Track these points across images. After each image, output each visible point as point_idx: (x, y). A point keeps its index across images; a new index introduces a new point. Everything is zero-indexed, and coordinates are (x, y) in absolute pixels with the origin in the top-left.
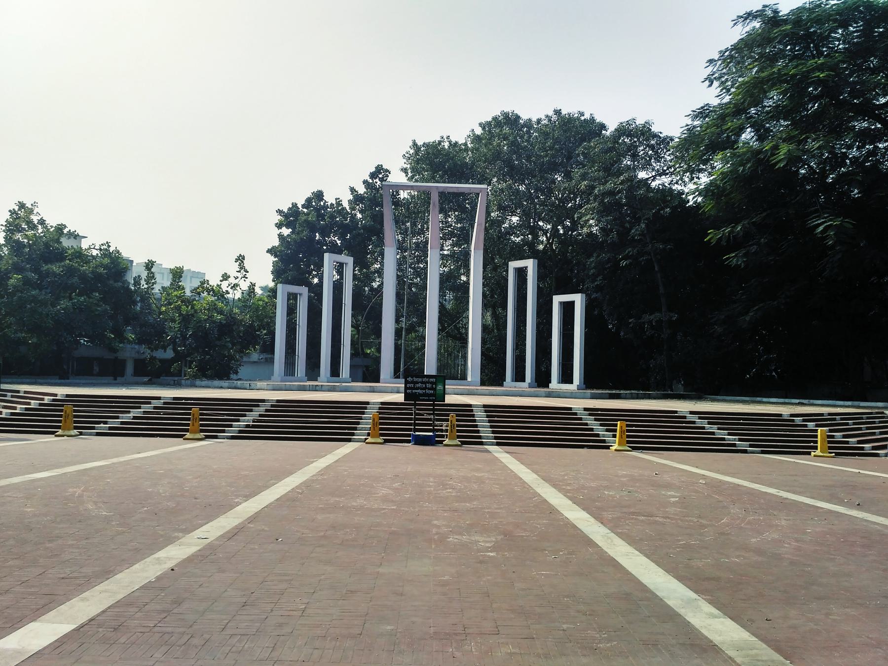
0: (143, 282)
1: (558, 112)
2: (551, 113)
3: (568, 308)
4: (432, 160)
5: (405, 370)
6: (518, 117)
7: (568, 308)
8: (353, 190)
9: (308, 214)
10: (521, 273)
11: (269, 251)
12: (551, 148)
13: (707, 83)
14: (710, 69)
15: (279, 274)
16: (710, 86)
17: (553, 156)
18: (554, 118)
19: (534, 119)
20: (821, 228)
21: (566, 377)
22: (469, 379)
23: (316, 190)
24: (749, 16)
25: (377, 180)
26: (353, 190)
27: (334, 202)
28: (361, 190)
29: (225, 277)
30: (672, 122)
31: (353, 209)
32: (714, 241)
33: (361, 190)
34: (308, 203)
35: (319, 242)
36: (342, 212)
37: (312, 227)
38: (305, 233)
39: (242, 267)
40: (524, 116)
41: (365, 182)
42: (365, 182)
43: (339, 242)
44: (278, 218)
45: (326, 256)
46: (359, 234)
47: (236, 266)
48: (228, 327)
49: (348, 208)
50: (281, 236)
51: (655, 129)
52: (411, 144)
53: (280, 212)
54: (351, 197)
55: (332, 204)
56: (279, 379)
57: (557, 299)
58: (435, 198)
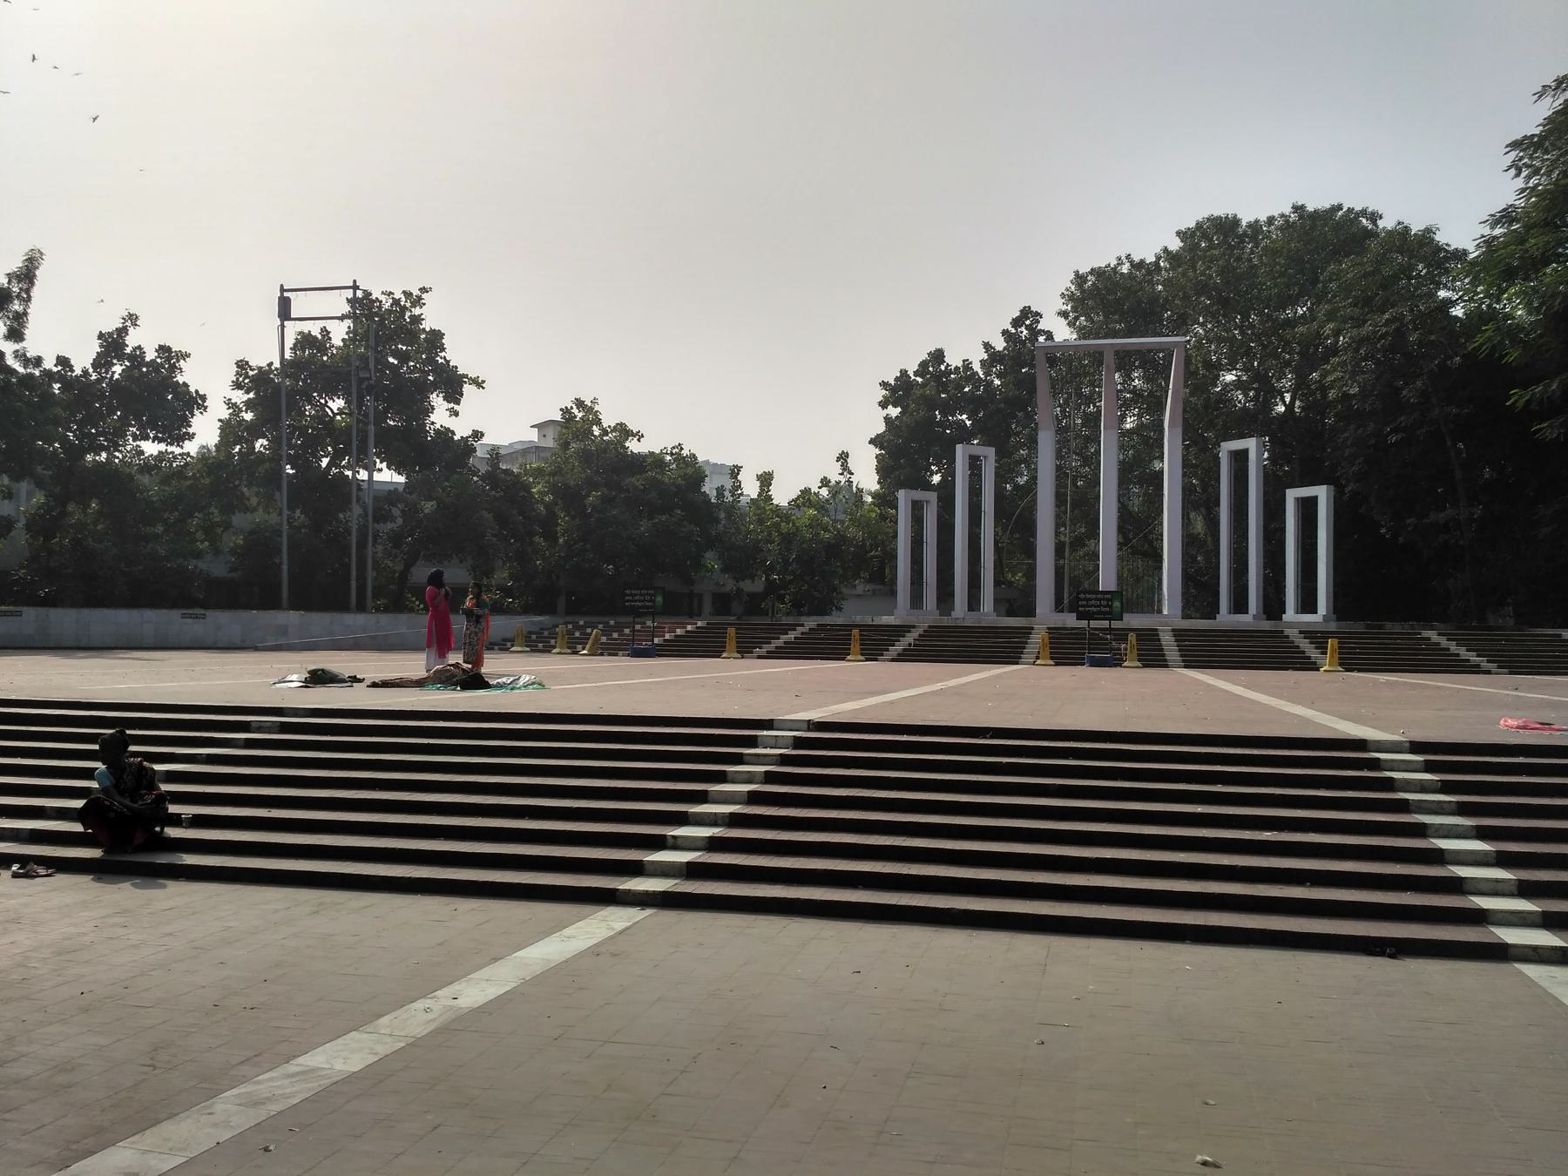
0: (727, 493)
1: (1298, 209)
2: (1287, 210)
3: (1308, 508)
4: (1108, 297)
6: (1235, 222)
8: (987, 346)
9: (923, 385)
10: (1240, 457)
11: (871, 442)
12: (1282, 275)
13: (1513, 172)
14: (1513, 155)
15: (884, 470)
16: (1518, 175)
17: (1288, 286)
18: (1293, 217)
19: (1263, 218)
22: (1165, 612)
26: (987, 346)
27: (960, 364)
28: (1000, 344)
29: (825, 482)
30: (1463, 231)
31: (987, 374)
33: (1000, 344)
34: (923, 369)
35: (940, 424)
37: (931, 403)
39: (845, 468)
40: (1246, 218)
41: (1005, 332)
42: (1005, 332)
43: (968, 423)
45: (959, 447)
47: (838, 467)
48: (835, 548)
50: (887, 419)
51: (1441, 238)
52: (1072, 276)
53: (884, 385)
55: (957, 368)
57: (1292, 495)
58: (1109, 359)
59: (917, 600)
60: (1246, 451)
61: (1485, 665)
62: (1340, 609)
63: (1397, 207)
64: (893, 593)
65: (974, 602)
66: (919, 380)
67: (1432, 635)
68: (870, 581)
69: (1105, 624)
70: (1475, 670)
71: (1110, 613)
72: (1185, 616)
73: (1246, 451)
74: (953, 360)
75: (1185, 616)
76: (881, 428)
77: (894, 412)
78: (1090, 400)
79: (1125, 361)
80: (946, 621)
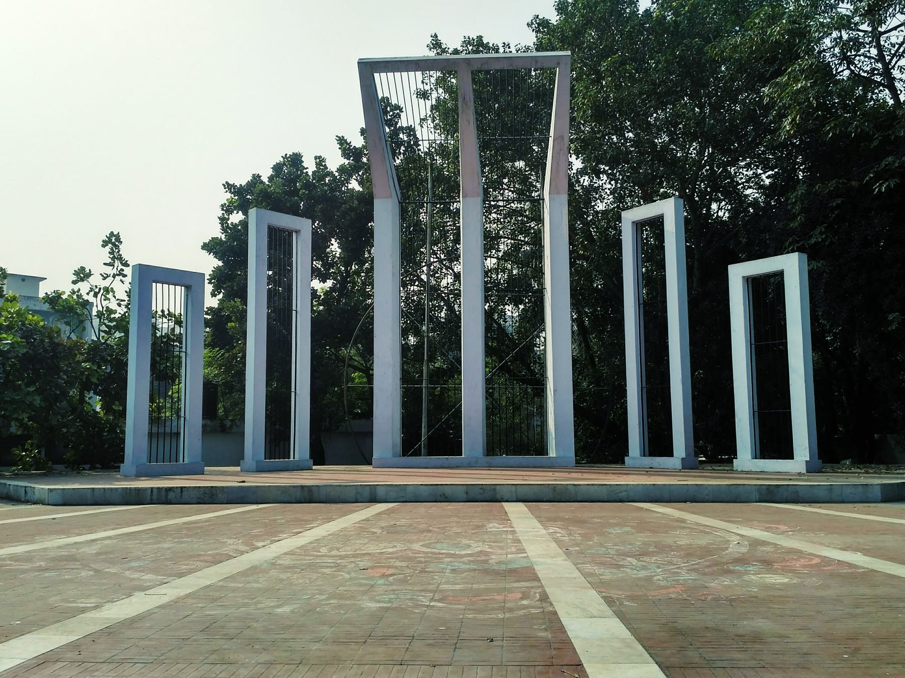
5: (429, 438)
8: (342, 141)
11: (205, 247)
21: (774, 440)
22: (552, 453)
23: (290, 153)
26: (342, 141)
29: (82, 275)
39: (116, 257)
44: (226, 197)
46: (352, 209)
47: (105, 254)
49: (337, 174)
53: (229, 187)
56: (133, 471)
74: (310, 166)
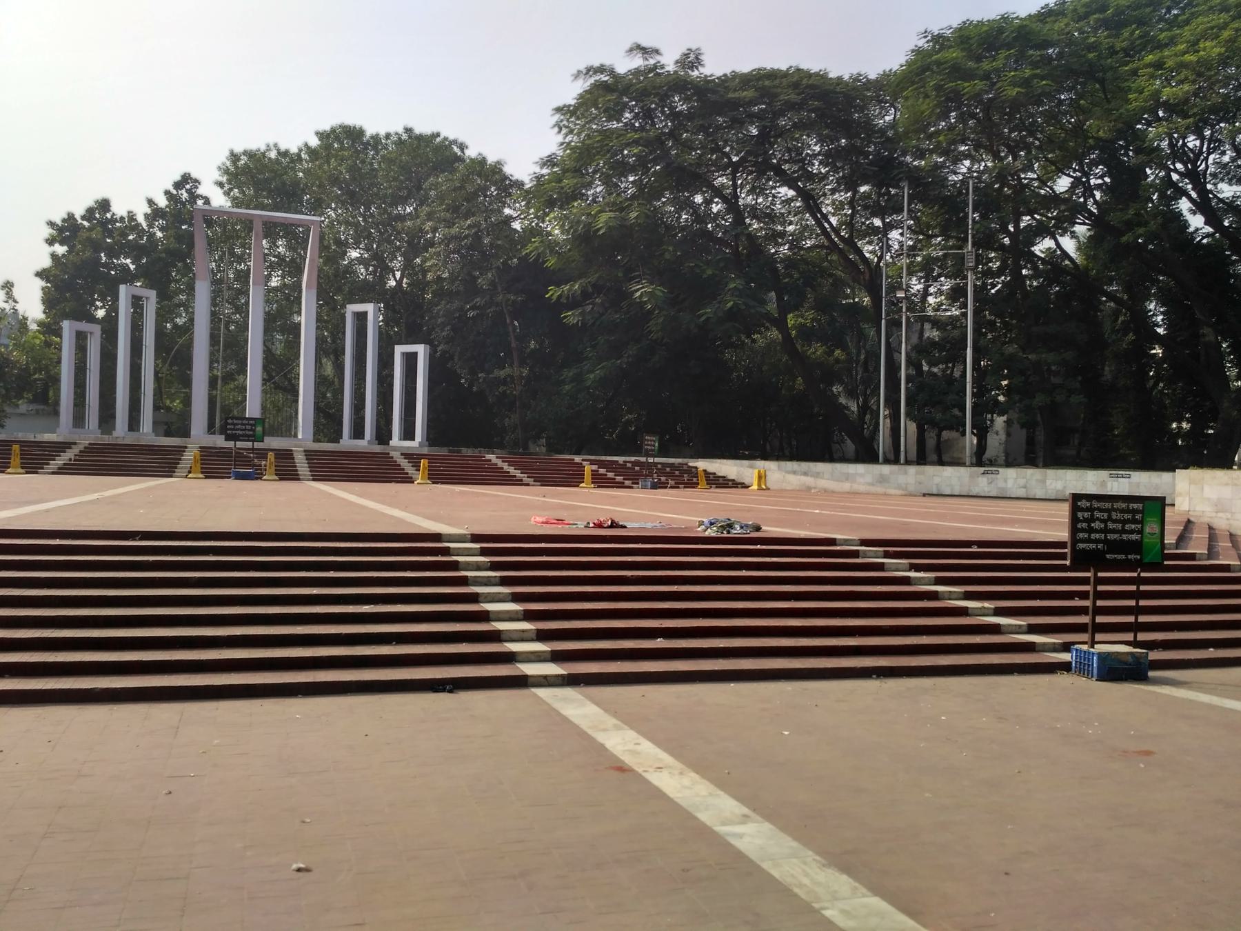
1: (408, 130)
2: (401, 130)
3: (411, 359)
4: (255, 174)
7: (411, 359)
8: (150, 202)
9: (90, 229)
10: (361, 317)
12: (395, 179)
13: (556, 129)
15: (50, 301)
18: (405, 137)
20: (638, 294)
22: (300, 436)
24: (590, 71)
25: (183, 191)
26: (150, 202)
27: (125, 215)
28: (162, 202)
30: (523, 166)
31: (151, 226)
32: (555, 297)
33: (162, 202)
35: (106, 265)
36: (136, 227)
37: (97, 246)
38: (88, 254)
39: (9, 296)
40: (370, 131)
41: (167, 193)
42: (167, 193)
43: (132, 267)
44: (47, 232)
45: (122, 288)
49: (144, 225)
50: (54, 256)
51: (508, 170)
52: (227, 153)
53: (51, 224)
54: (149, 211)
55: (122, 218)
57: (399, 350)
58: (258, 227)
59: (79, 419)
60: (366, 313)
61: (526, 480)
62: (433, 438)
63: (481, 143)
64: (56, 413)
65: (134, 424)
66: (86, 223)
67: (492, 458)
68: (34, 400)
69: (249, 445)
70: (519, 483)
71: (253, 436)
72: (316, 440)
73: (366, 313)
75: (316, 440)
76: (47, 263)
77: (61, 250)
78: (241, 259)
79: (271, 230)
80: (107, 439)
